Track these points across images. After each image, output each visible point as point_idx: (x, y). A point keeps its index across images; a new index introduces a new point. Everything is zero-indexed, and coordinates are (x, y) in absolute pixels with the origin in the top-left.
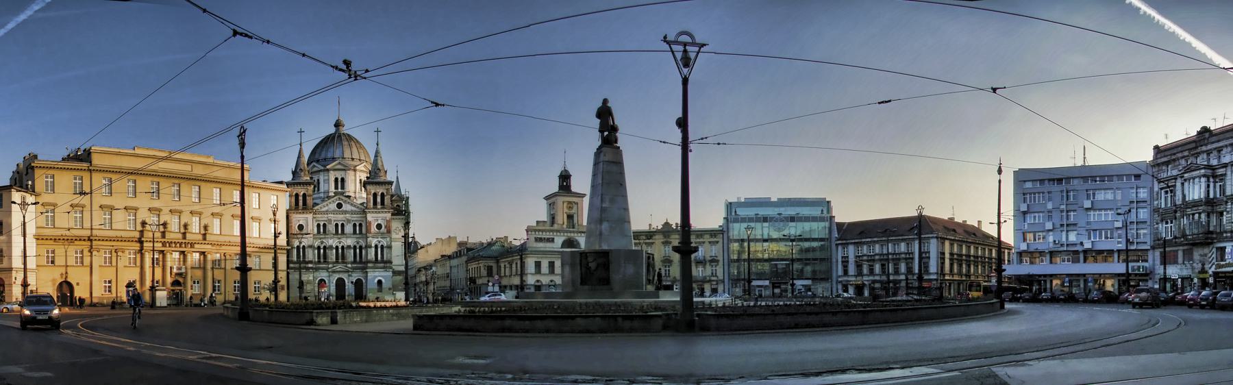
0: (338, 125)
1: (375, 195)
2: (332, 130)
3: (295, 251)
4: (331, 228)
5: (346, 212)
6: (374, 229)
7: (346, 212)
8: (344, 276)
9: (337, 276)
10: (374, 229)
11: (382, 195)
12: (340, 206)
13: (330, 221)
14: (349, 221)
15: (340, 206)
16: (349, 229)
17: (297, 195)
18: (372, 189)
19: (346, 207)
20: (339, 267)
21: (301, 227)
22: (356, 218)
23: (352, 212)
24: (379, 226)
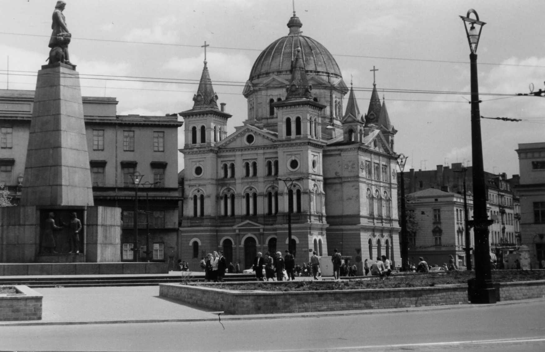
0: (294, 24)
1: (288, 121)
2: (286, 31)
3: (191, 203)
4: (240, 171)
5: (257, 148)
7: (257, 148)
11: (298, 120)
12: (250, 139)
15: (250, 139)
16: (262, 170)
17: (194, 129)
19: (257, 141)
21: (198, 171)
22: (269, 153)
23: (264, 147)
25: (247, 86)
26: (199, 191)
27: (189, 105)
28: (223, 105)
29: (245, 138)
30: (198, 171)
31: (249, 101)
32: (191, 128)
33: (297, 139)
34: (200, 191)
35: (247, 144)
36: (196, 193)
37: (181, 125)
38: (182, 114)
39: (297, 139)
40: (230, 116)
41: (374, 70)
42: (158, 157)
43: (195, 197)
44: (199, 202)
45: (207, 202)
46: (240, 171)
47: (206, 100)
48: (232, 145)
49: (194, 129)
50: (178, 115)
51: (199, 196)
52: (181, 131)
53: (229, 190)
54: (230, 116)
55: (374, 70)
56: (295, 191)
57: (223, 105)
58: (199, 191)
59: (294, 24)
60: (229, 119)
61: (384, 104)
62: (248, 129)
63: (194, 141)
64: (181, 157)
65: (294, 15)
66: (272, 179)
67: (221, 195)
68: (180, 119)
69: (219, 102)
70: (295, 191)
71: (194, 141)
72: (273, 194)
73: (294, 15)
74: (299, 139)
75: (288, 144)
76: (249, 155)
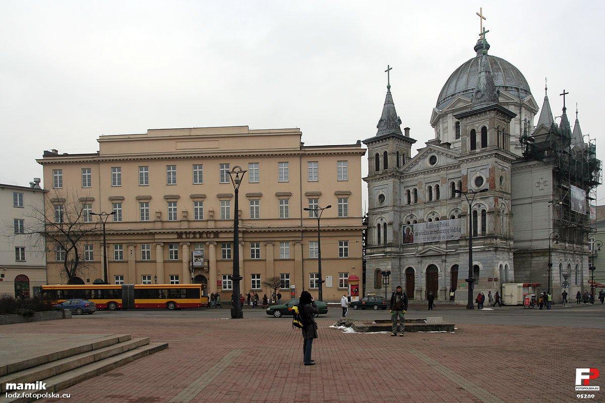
3: (376, 231)
4: (423, 195)
5: (439, 169)
6: (472, 185)
7: (439, 169)
8: (437, 262)
9: (428, 262)
10: (472, 185)
12: (433, 160)
13: (420, 183)
14: (444, 180)
15: (433, 160)
16: (445, 192)
17: (377, 155)
18: (468, 125)
19: (441, 161)
21: (382, 197)
23: (448, 168)
24: (479, 181)
25: (434, 113)
26: (382, 219)
27: (373, 133)
28: (407, 129)
29: (427, 160)
30: (382, 197)
31: (436, 130)
32: (374, 155)
33: (482, 152)
34: (384, 220)
35: (429, 165)
37: (364, 154)
38: (365, 142)
39: (482, 152)
42: (343, 187)
43: (379, 225)
44: (382, 230)
45: (390, 230)
46: (423, 195)
47: (391, 127)
48: (414, 169)
49: (377, 155)
50: (362, 143)
51: (382, 224)
52: (365, 160)
53: (412, 216)
56: (479, 212)
57: (407, 129)
58: (382, 219)
62: (431, 149)
63: (378, 169)
64: (365, 185)
66: (456, 201)
67: (404, 222)
68: (364, 146)
69: (402, 127)
70: (479, 212)
71: (378, 169)
74: (484, 151)
75: (472, 159)
76: (434, 177)
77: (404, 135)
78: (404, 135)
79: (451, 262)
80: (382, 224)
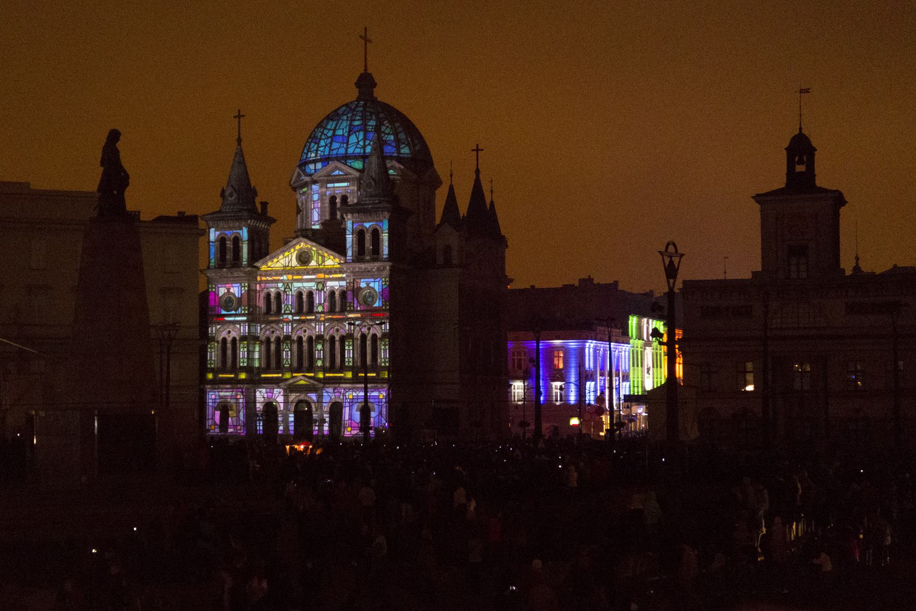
0: (366, 82)
4: (289, 302)
20: (301, 379)
28: (264, 205)
36: (224, 334)
40: (274, 221)
41: (477, 150)
46: (289, 302)
54: (274, 221)
55: (477, 150)
59: (366, 82)
60: (274, 225)
61: (492, 204)
65: (366, 69)
69: (258, 200)
72: (337, 338)
73: (366, 69)
77: (259, 210)
78: (259, 210)
79: (329, 395)
80: (229, 339)
